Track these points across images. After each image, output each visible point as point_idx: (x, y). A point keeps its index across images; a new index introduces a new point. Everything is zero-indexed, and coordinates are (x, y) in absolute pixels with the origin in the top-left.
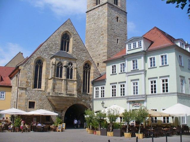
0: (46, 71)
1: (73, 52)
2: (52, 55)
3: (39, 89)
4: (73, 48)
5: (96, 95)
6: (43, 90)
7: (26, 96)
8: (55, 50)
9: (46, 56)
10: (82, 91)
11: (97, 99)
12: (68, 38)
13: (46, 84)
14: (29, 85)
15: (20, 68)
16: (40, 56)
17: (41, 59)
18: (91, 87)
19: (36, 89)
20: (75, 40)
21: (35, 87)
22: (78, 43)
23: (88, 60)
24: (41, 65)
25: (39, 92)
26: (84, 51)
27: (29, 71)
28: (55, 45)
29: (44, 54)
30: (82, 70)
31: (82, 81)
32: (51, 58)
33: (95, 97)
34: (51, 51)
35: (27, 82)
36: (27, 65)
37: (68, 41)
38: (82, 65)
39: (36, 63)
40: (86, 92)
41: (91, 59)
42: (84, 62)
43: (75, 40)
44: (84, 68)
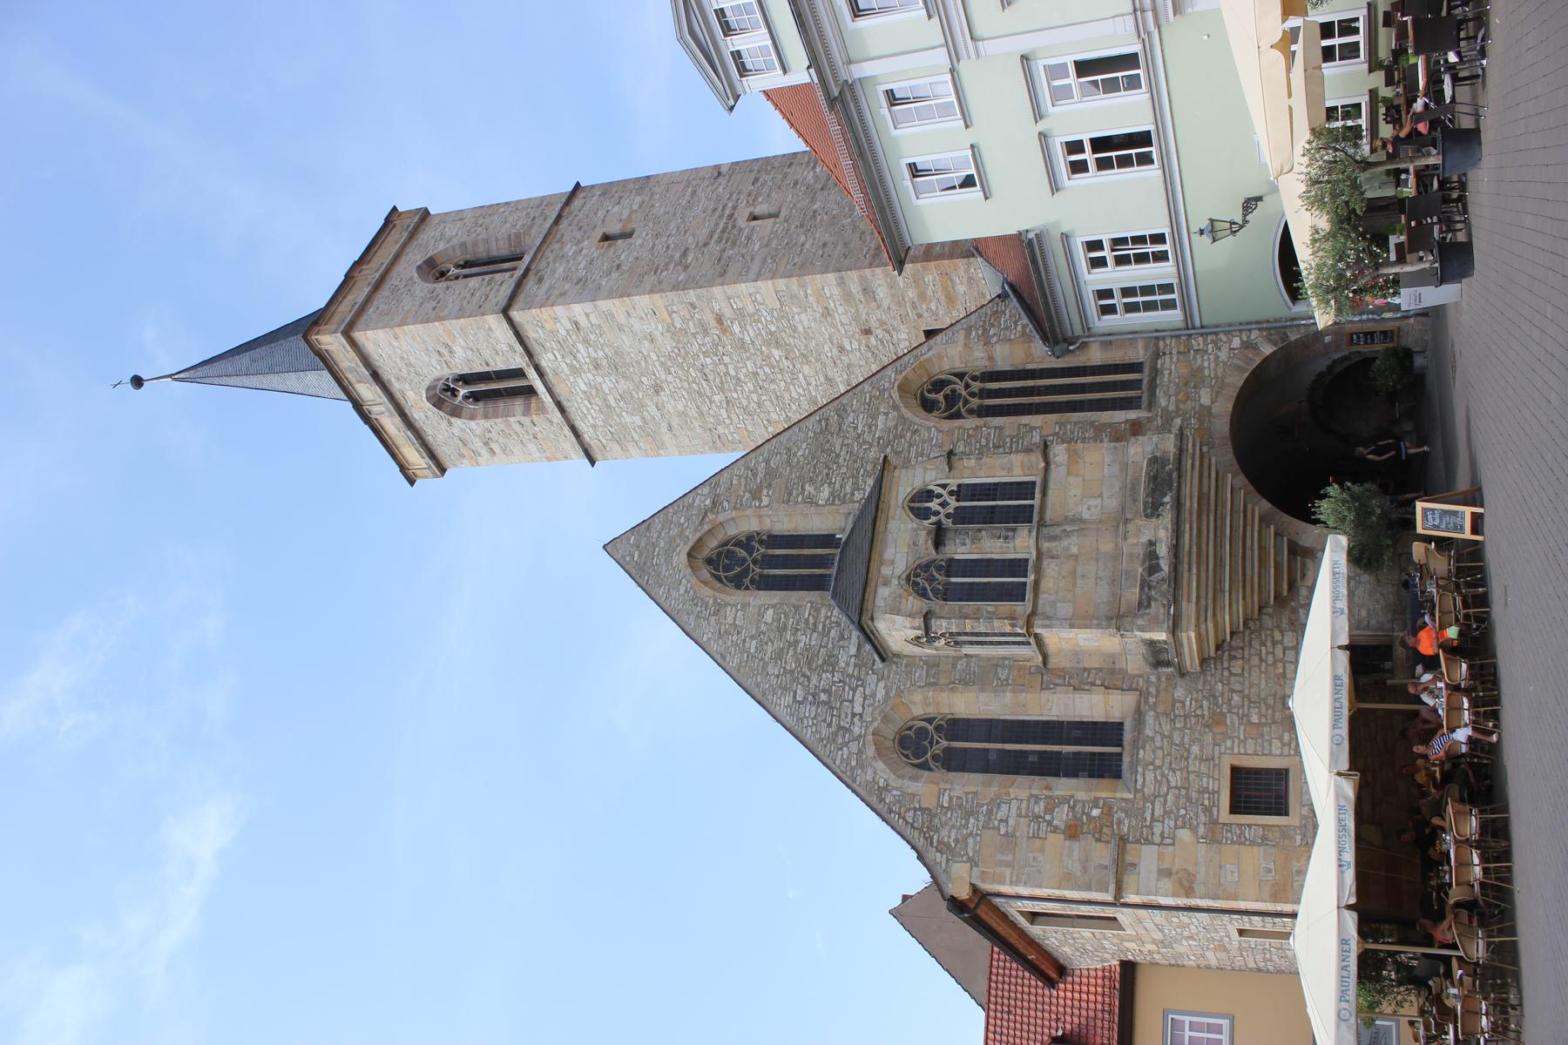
0: (981, 691)
2: (859, 649)
3: (1128, 736)
5: (1150, 306)
6: (1134, 705)
7: (1184, 834)
8: (825, 633)
9: (874, 695)
10: (1132, 415)
11: (1185, 297)
12: (739, 544)
13: (1079, 679)
14: (1096, 812)
15: (963, 893)
16: (870, 737)
17: (890, 731)
18: (1095, 355)
19: (1126, 759)
21: (1106, 768)
23: (896, 395)
24: (938, 728)
25: (1148, 732)
26: (834, 428)
27: (989, 812)
28: (788, 636)
29: (858, 709)
30: (971, 422)
31: (1055, 417)
32: (883, 653)
33: (1174, 316)
34: (831, 663)
35: (1072, 832)
36: (944, 833)
37: (761, 542)
38: (934, 429)
39: (924, 766)
40: (1135, 385)
41: (890, 372)
42: (908, 415)
44: (958, 416)
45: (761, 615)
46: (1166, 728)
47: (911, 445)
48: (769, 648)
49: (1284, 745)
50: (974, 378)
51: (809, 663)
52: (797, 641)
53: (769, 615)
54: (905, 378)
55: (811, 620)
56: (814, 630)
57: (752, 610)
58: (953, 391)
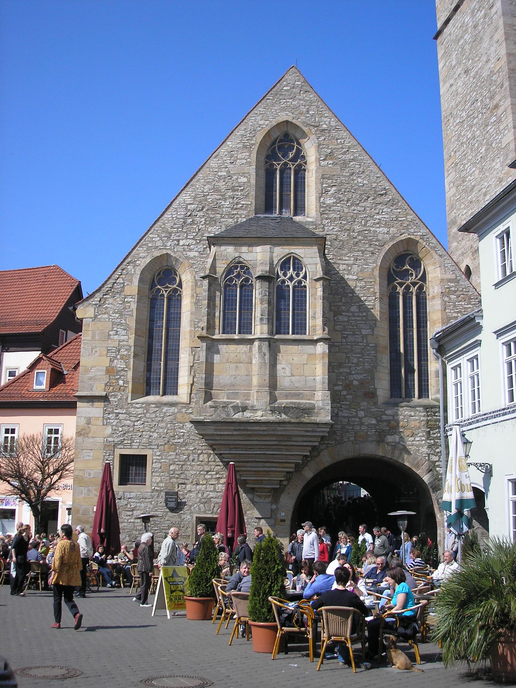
1: (324, 210)
4: (322, 193)
20: (329, 156)
22: (345, 164)
25: (165, 409)
28: (230, 193)
34: (212, 222)
43: (329, 156)
45: (243, 175)
46: (168, 419)
47: (363, 252)
48: (221, 184)
49: (158, 483)
50: (421, 288)
51: (212, 209)
52: (225, 200)
53: (244, 180)
54: (417, 242)
55: (239, 206)
56: (232, 209)
57: (246, 169)
58: (412, 275)
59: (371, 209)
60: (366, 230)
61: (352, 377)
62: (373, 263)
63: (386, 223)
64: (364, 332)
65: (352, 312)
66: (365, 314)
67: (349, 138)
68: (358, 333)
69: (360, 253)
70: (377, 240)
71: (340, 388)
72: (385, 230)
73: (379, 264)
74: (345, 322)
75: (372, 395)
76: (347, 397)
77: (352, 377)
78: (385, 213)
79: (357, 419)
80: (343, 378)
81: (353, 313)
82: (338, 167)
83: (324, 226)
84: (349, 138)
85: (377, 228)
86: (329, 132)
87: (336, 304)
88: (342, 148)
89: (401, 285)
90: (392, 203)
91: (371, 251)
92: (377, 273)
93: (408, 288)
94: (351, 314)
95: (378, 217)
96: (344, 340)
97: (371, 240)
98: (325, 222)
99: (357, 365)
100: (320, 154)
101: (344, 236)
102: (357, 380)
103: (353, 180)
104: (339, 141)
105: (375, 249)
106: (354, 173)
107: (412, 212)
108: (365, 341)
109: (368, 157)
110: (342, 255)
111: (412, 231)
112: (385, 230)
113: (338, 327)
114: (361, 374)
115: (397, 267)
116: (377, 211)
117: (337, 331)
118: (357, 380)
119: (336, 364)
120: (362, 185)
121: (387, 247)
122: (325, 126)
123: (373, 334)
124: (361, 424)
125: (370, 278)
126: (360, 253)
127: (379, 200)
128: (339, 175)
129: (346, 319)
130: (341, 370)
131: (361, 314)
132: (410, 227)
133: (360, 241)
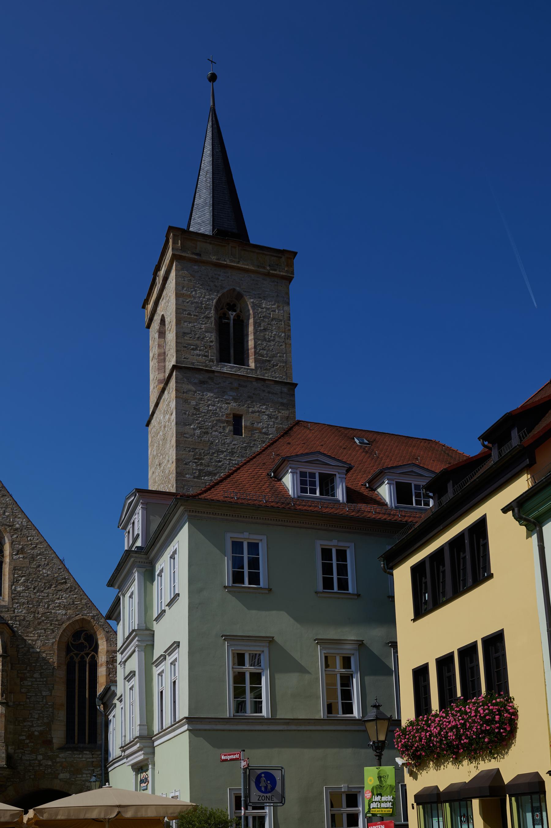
4: (14, 582)
20: (21, 551)
22: (33, 558)
43: (21, 551)
47: (45, 630)
59: (53, 595)
60: (48, 612)
61: (33, 729)
62: (53, 639)
63: (64, 606)
64: (44, 694)
65: (35, 678)
66: (45, 679)
67: (38, 536)
68: (39, 694)
69: (43, 631)
70: (57, 620)
71: (24, 738)
72: (64, 612)
73: (57, 639)
74: (29, 685)
75: (49, 743)
76: (29, 745)
77: (33, 729)
78: (65, 598)
79: (37, 762)
80: (27, 730)
81: (36, 678)
82: (27, 560)
83: (15, 609)
84: (38, 536)
85: (57, 610)
86: (21, 531)
87: (22, 672)
88: (31, 544)
89: (77, 655)
90: (71, 590)
91: (52, 629)
92: (56, 647)
93: (82, 657)
94: (34, 680)
95: (58, 601)
96: (28, 700)
97: (52, 620)
98: (16, 606)
99: (38, 719)
100: (13, 550)
101: (30, 617)
102: (38, 731)
103: (40, 571)
104: (29, 538)
105: (55, 627)
106: (40, 565)
107: (86, 597)
108: (44, 701)
109: (52, 551)
110: (28, 632)
111: (86, 612)
112: (64, 612)
113: (23, 690)
114: (41, 726)
115: (74, 641)
116: (58, 596)
117: (23, 693)
118: (38, 731)
119: (21, 719)
120: (46, 575)
121: (64, 626)
122: (17, 526)
123: (51, 695)
124: (40, 765)
125: (50, 651)
126: (43, 631)
127: (60, 587)
128: (28, 567)
129: (30, 684)
130: (25, 724)
131: (42, 680)
132: (84, 609)
133: (43, 621)
